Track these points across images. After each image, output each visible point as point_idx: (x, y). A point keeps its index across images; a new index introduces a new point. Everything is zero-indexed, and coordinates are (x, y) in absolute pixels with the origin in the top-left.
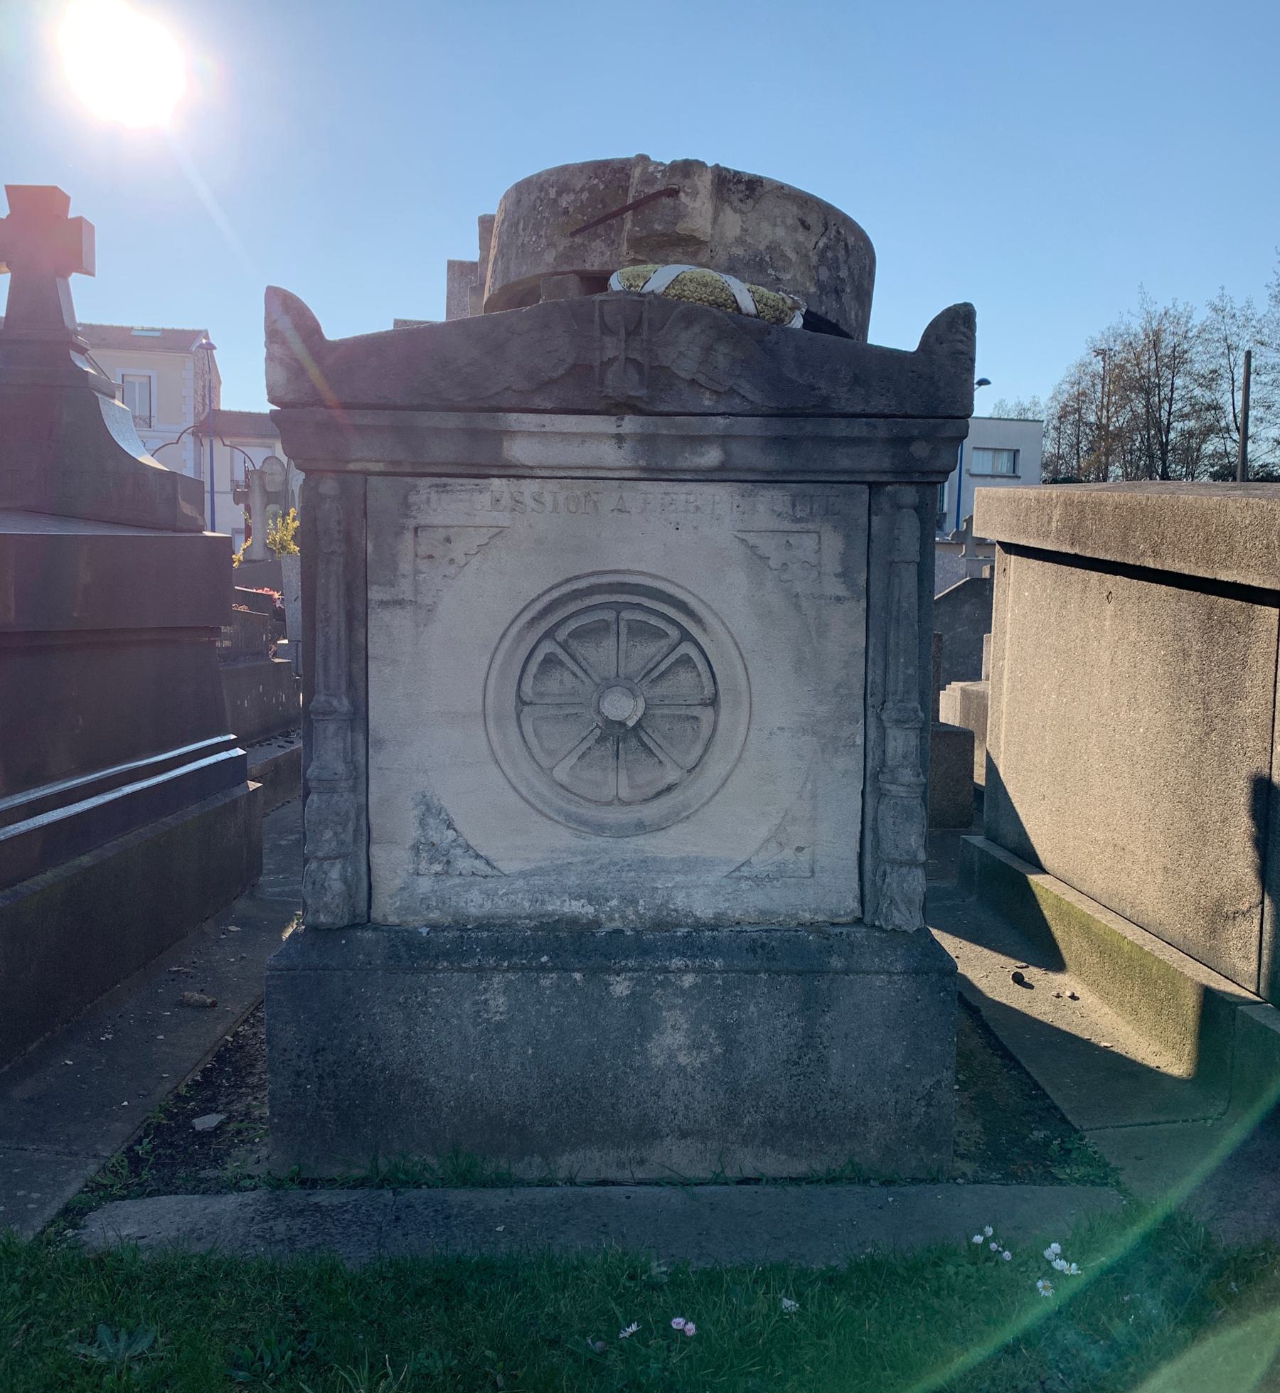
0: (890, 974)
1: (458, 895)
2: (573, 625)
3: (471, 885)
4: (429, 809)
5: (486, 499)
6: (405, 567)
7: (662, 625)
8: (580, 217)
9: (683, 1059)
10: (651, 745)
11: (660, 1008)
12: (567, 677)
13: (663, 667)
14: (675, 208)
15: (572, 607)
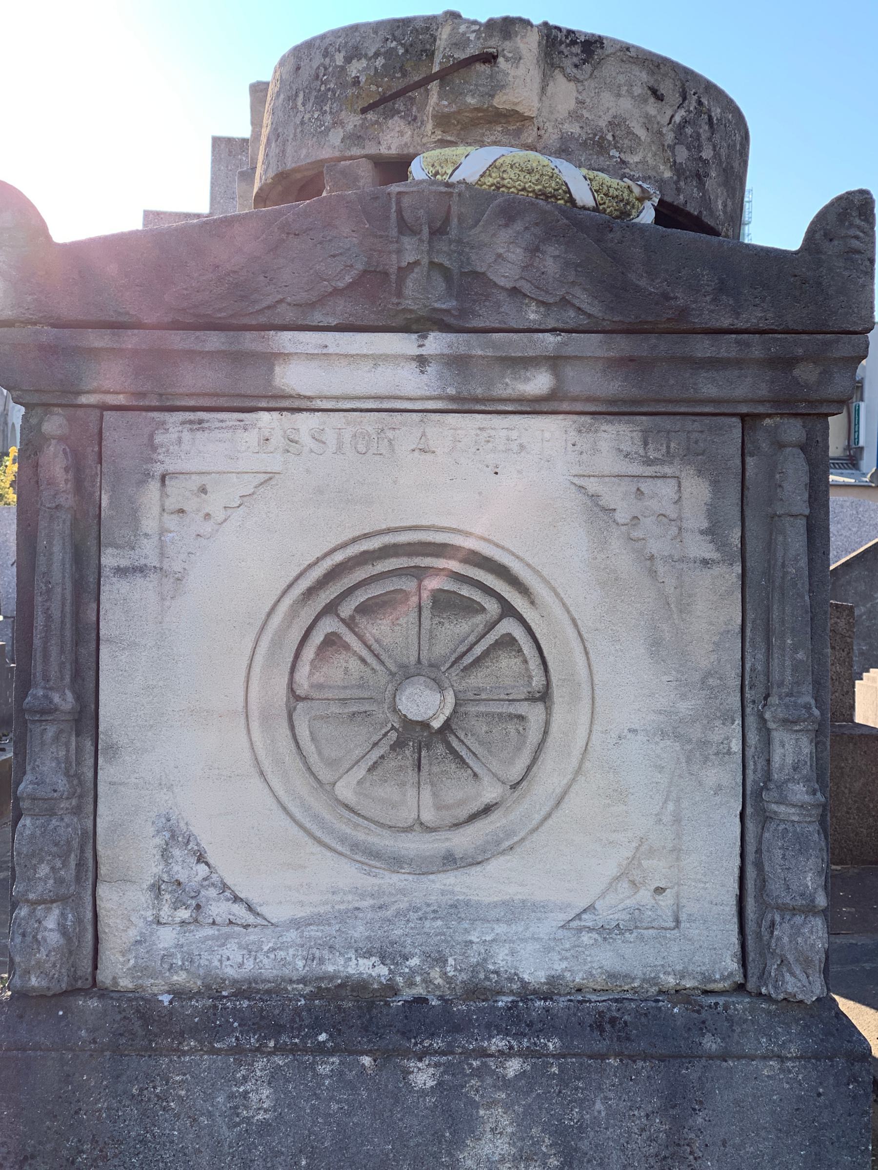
0: (781, 1059)
2: (361, 597)
3: (228, 937)
4: (175, 837)
5: (251, 438)
6: (149, 524)
7: (477, 596)
10: (463, 753)
11: (476, 1106)
12: (354, 664)
13: (478, 650)
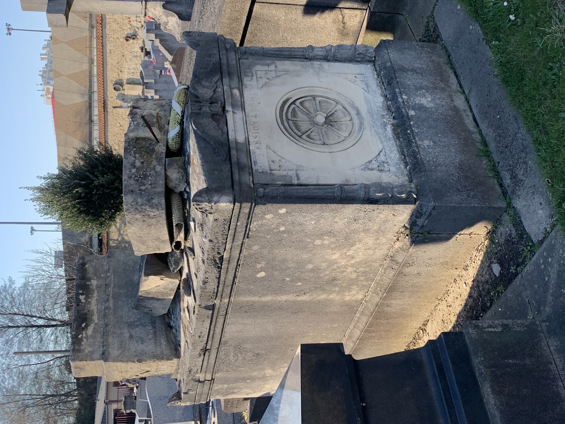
0: (388, 53)
1: (393, 160)
2: (296, 131)
3: (389, 156)
4: (367, 167)
5: (258, 151)
6: (285, 173)
8: (145, 157)
9: (430, 99)
10: (331, 113)
11: (415, 104)
12: (312, 134)
13: (304, 110)
14: (148, 116)
15: (290, 131)
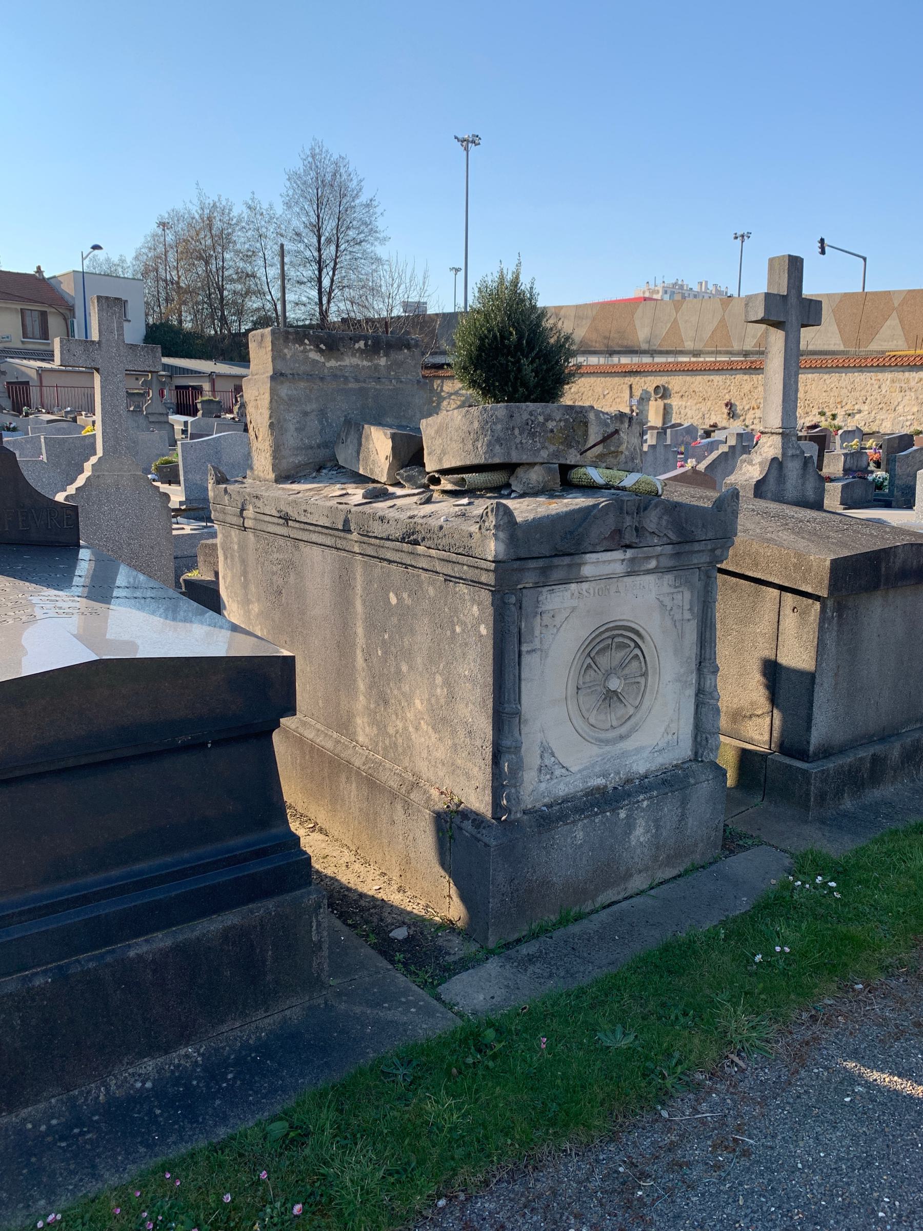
0: (708, 780)
2: (597, 648)
4: (546, 750)
5: (567, 594)
6: (537, 633)
7: (628, 642)
9: (642, 839)
11: (635, 819)
12: (592, 672)
13: (627, 661)
15: (598, 640)
